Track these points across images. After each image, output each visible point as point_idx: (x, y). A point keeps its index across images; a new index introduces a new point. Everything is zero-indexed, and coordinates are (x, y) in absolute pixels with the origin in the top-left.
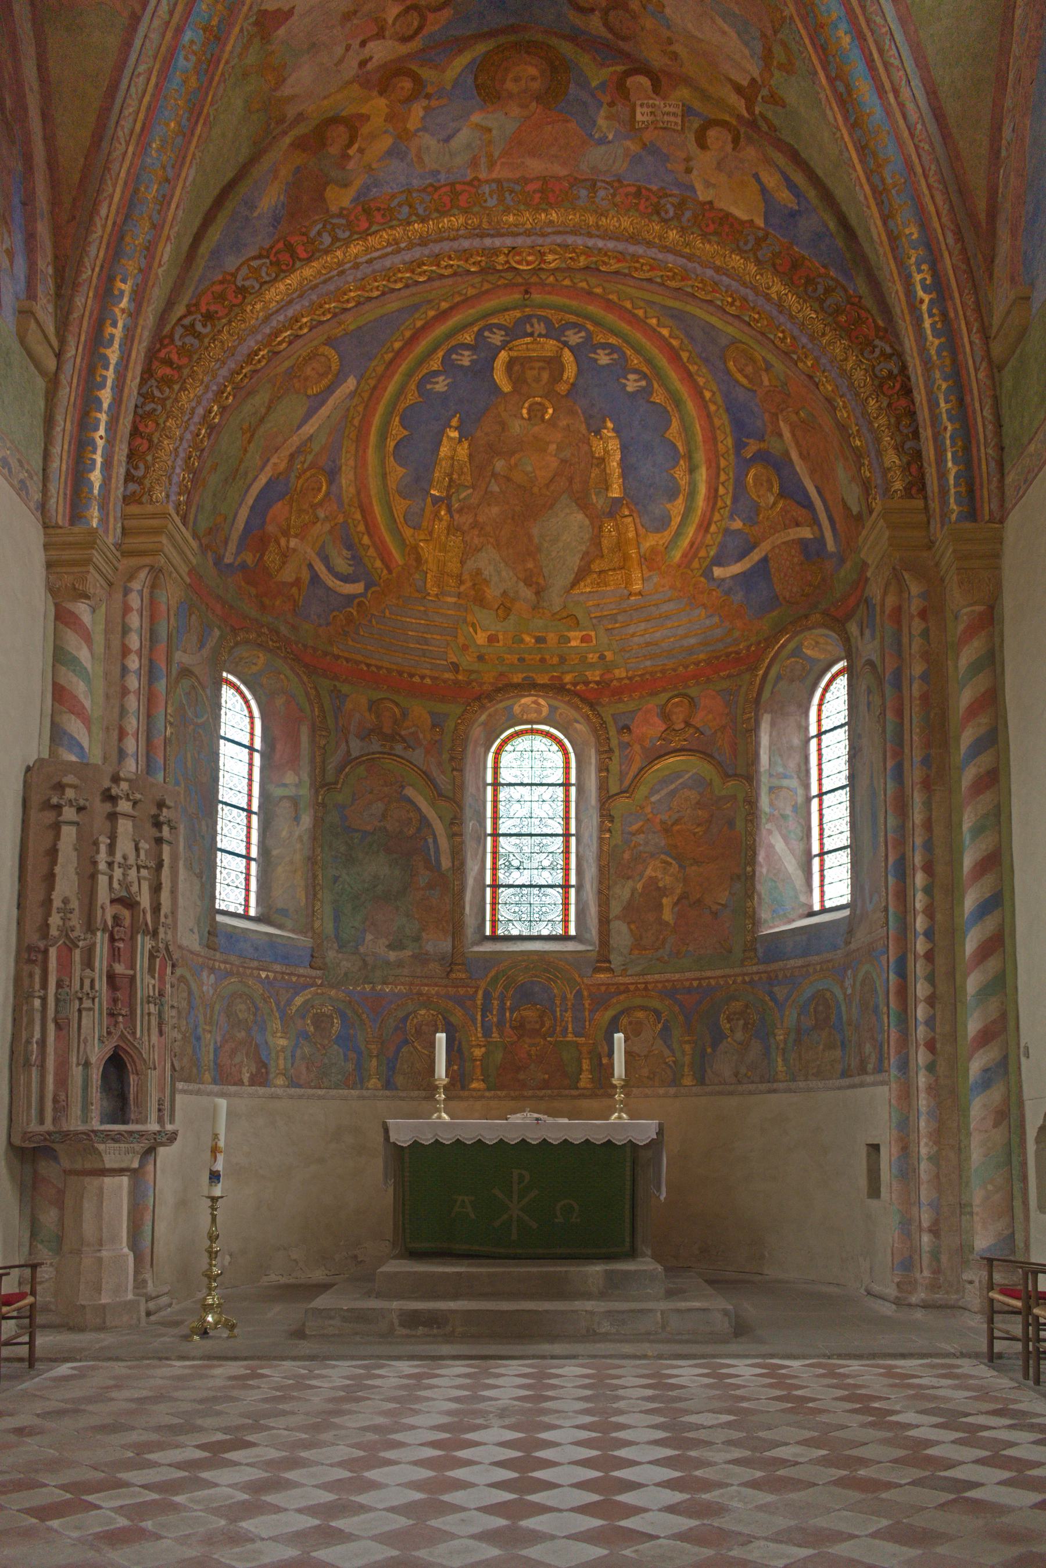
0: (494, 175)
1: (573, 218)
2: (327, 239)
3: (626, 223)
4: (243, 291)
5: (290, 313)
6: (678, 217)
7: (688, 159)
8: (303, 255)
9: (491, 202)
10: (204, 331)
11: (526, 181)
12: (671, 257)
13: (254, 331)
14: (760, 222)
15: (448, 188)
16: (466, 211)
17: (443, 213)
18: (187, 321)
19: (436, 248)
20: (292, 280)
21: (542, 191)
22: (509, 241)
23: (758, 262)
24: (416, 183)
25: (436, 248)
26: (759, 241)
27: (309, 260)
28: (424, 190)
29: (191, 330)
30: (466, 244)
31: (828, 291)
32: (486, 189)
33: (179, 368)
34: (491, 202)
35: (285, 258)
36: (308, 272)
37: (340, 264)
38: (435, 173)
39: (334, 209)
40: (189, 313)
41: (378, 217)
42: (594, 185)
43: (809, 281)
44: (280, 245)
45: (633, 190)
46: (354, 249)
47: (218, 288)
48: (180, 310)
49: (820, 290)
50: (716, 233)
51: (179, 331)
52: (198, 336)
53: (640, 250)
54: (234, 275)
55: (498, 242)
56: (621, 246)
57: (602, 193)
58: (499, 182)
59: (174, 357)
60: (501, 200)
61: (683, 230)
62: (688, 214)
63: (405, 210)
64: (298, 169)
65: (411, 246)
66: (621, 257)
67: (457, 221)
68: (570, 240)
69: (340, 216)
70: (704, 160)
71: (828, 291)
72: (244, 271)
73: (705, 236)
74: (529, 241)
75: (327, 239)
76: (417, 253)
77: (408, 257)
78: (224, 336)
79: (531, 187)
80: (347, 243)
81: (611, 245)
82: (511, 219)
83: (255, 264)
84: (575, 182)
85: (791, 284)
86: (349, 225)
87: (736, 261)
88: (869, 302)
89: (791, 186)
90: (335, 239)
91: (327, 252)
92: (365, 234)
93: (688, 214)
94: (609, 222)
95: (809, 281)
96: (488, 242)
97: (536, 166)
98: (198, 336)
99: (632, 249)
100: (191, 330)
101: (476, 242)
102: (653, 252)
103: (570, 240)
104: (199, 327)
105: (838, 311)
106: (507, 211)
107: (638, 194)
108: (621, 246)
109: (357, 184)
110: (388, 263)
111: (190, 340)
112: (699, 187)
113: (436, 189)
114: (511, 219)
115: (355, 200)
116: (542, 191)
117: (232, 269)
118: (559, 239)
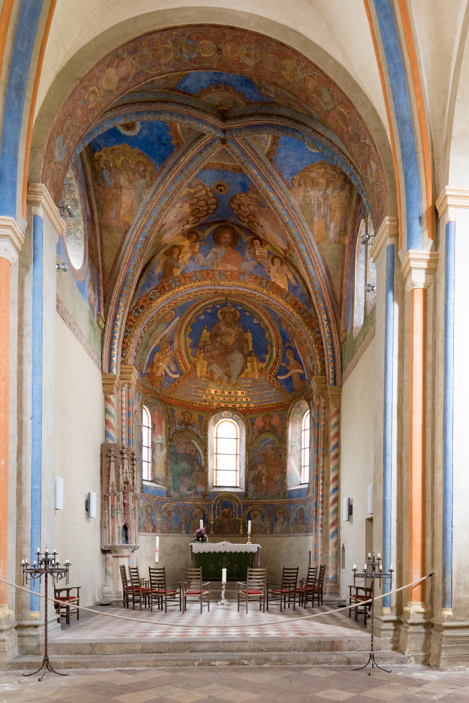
0: (218, 269)
1: (239, 284)
2: (174, 285)
3: (253, 286)
4: (151, 299)
5: (163, 305)
6: (266, 286)
7: (269, 268)
8: (167, 289)
9: (218, 277)
10: (141, 311)
11: (226, 271)
12: (264, 296)
13: (154, 311)
14: (287, 289)
15: (205, 272)
16: (211, 279)
17: (205, 280)
18: (136, 308)
19: (203, 288)
20: (165, 297)
21: (231, 275)
22: (222, 288)
23: (287, 302)
24: (197, 269)
25: (203, 288)
26: (287, 295)
27: (169, 291)
28: (199, 272)
29: (137, 310)
30: (211, 287)
31: (304, 312)
32: (216, 273)
33: (134, 322)
34: (218, 277)
35: (162, 290)
36: (168, 294)
37: (177, 292)
38: (203, 266)
39: (175, 276)
40: (136, 305)
41: (187, 280)
42: (244, 275)
43: (300, 309)
44: (161, 286)
45: (254, 277)
46: (181, 288)
47: (144, 298)
48: (134, 304)
49: (302, 311)
50: (276, 292)
51: (134, 311)
52: (139, 313)
53: (257, 293)
54: (148, 294)
55: (219, 288)
56: (251, 292)
57: (247, 277)
58: (219, 271)
59: (133, 319)
60: (220, 277)
61: (267, 290)
62: (269, 285)
63: (195, 277)
64: (165, 262)
65: (196, 287)
66: (251, 293)
67: (209, 282)
68: (238, 288)
69: (177, 278)
70: (273, 269)
71: (304, 312)
72: (151, 293)
73: (273, 293)
74: (227, 288)
75: (174, 285)
76: (197, 289)
77: (195, 290)
78: (146, 313)
79: (228, 274)
80: (179, 286)
81: (249, 291)
82: (223, 283)
83: (154, 291)
84: (240, 273)
85: (294, 309)
86: (180, 281)
87: (281, 300)
88: (314, 316)
89: (295, 279)
90: (176, 285)
91: (174, 289)
92: (184, 284)
93: (269, 285)
94: (249, 286)
95: (300, 309)
96: (216, 287)
97: (230, 267)
98: (139, 313)
99: (254, 292)
100: (137, 310)
101: (214, 287)
102: (259, 294)
103: (238, 288)
104: (139, 310)
105: (306, 318)
106: (221, 280)
107: (256, 278)
108: (251, 292)
109: (182, 268)
110: (190, 291)
111: (137, 314)
112: (272, 277)
113: (203, 272)
114: (223, 283)
115: (181, 273)
116: (231, 275)
117: (148, 292)
118: (235, 288)
